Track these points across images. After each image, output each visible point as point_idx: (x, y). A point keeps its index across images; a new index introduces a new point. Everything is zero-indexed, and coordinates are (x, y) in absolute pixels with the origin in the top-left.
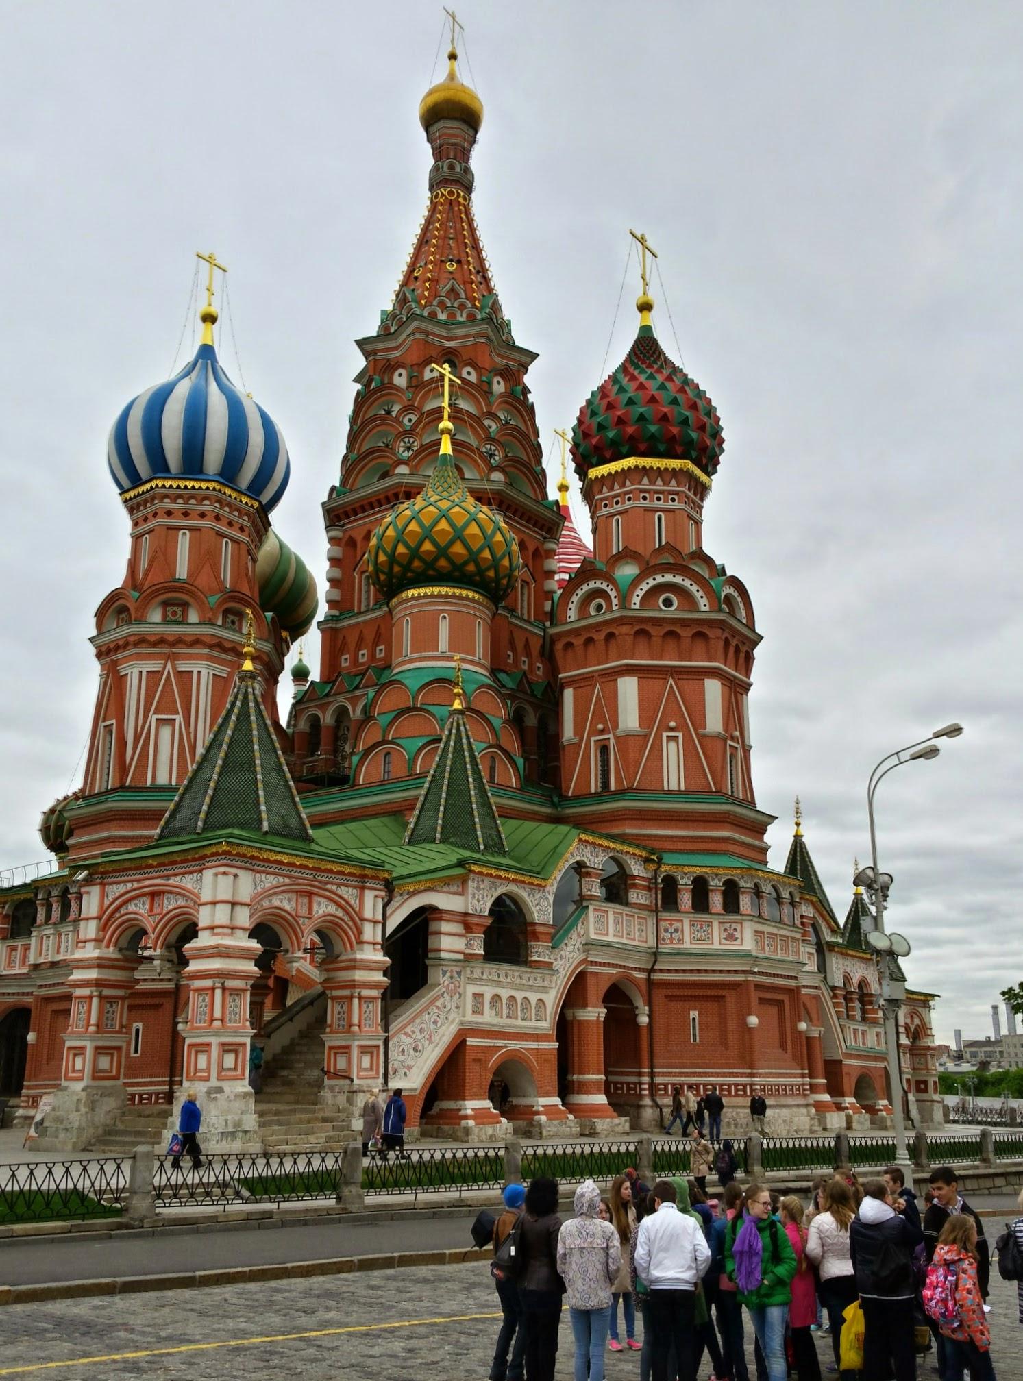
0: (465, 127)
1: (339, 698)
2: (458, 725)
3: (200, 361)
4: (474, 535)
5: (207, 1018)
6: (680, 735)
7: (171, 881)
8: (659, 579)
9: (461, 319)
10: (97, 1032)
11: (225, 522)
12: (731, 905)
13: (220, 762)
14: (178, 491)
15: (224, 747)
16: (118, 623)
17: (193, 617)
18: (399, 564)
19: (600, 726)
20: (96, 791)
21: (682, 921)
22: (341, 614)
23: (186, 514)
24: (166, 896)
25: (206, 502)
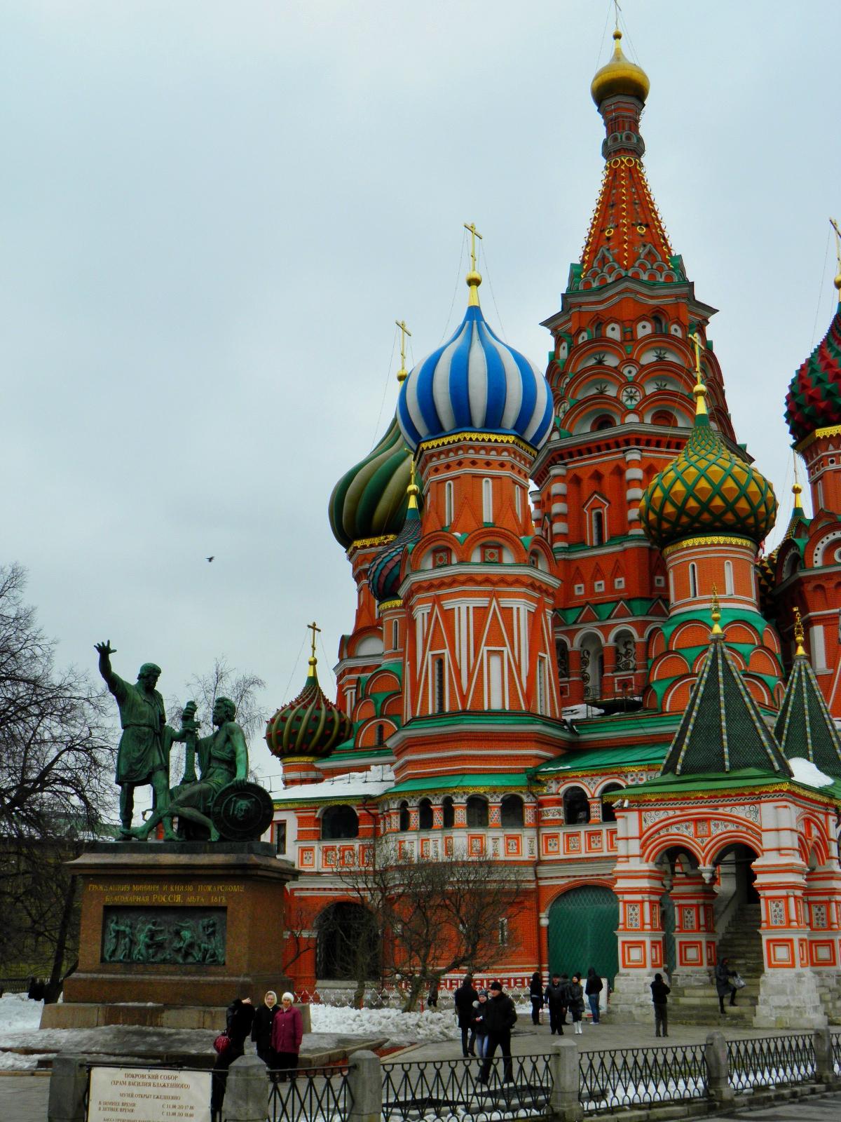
0: (637, 102)
2: (806, 669)
3: (475, 322)
4: (756, 492)
5: (784, 919)
7: (720, 810)
9: (662, 280)
10: (652, 929)
11: (517, 470)
13: (723, 711)
15: (722, 698)
18: (688, 515)
20: (430, 713)
23: (488, 464)
24: (712, 823)
25: (505, 453)
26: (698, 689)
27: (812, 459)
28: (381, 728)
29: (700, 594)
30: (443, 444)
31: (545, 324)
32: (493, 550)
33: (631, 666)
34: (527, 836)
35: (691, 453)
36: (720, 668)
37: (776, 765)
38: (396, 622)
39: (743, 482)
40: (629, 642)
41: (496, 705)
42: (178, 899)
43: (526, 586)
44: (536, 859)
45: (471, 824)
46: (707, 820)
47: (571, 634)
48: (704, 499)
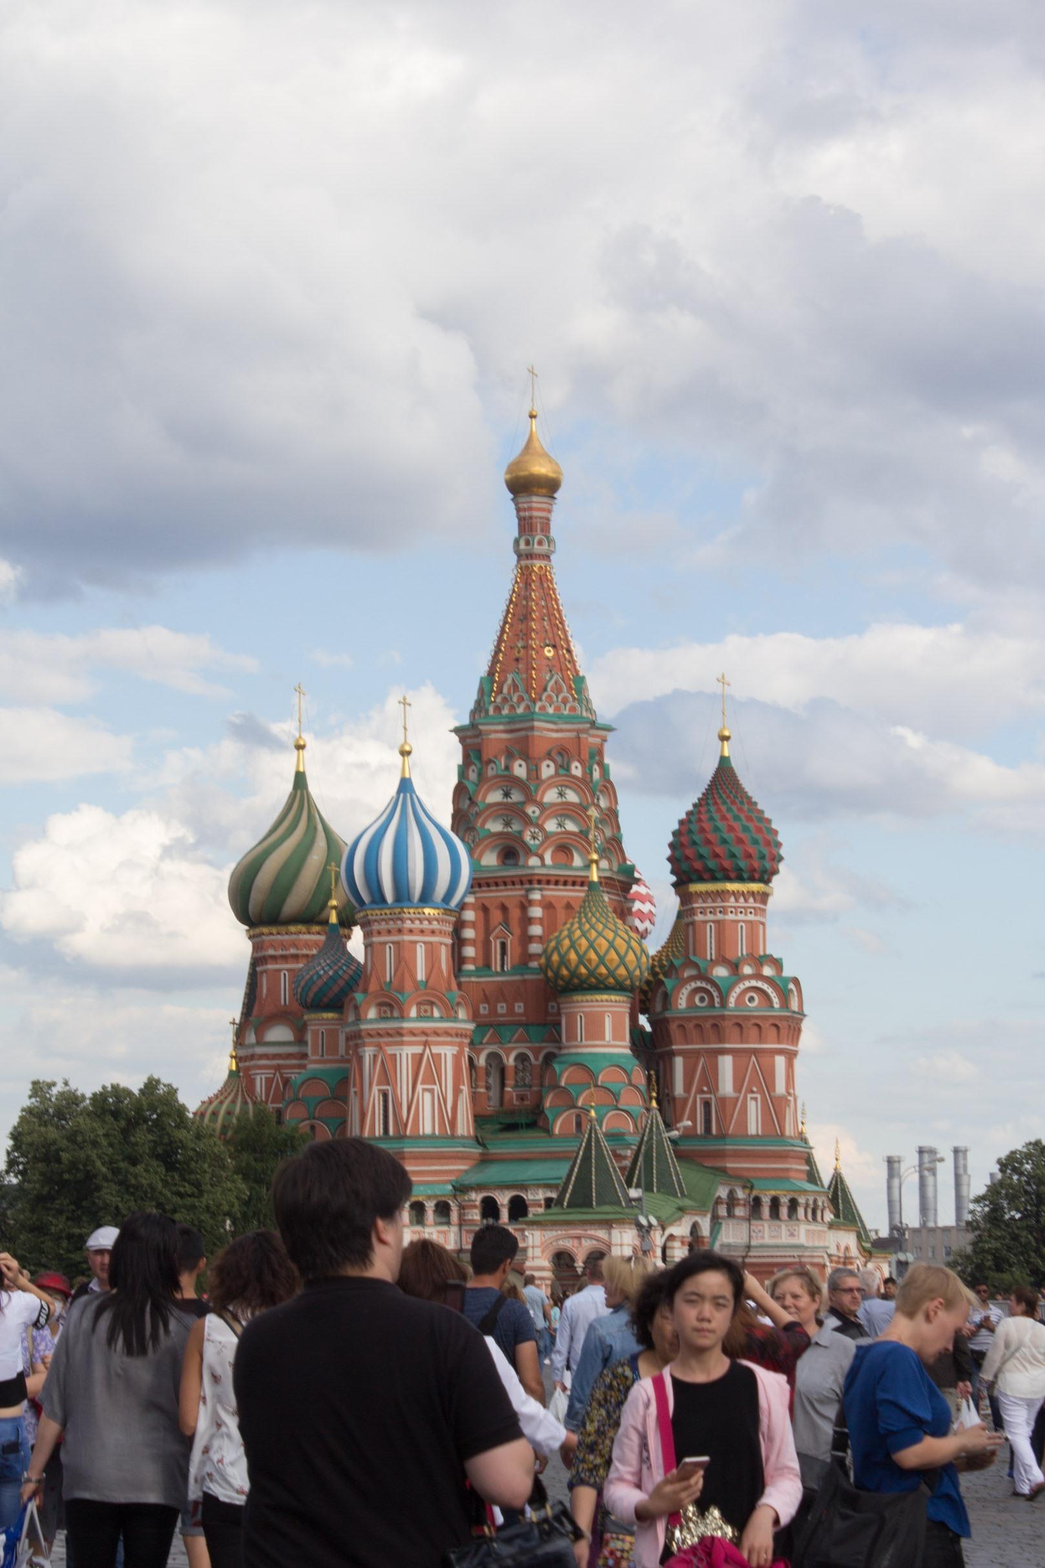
1: (492, 1047)
3: (408, 795)
4: (631, 961)
6: (759, 1096)
7: (589, 1232)
8: (747, 984)
9: (566, 712)
14: (418, 916)
16: (379, 1013)
17: (436, 1014)
18: (578, 978)
19: (705, 1089)
21: (763, 1226)
22: (476, 967)
23: (422, 931)
25: (435, 923)
26: (578, 1153)
27: (687, 905)
28: (313, 1127)
29: (586, 1040)
30: (386, 914)
31: (451, 731)
33: (527, 1081)
35: (584, 920)
36: (593, 1140)
38: (323, 1032)
39: (622, 953)
40: (526, 1060)
41: (428, 1130)
43: (451, 1035)
46: (579, 1238)
48: (591, 968)
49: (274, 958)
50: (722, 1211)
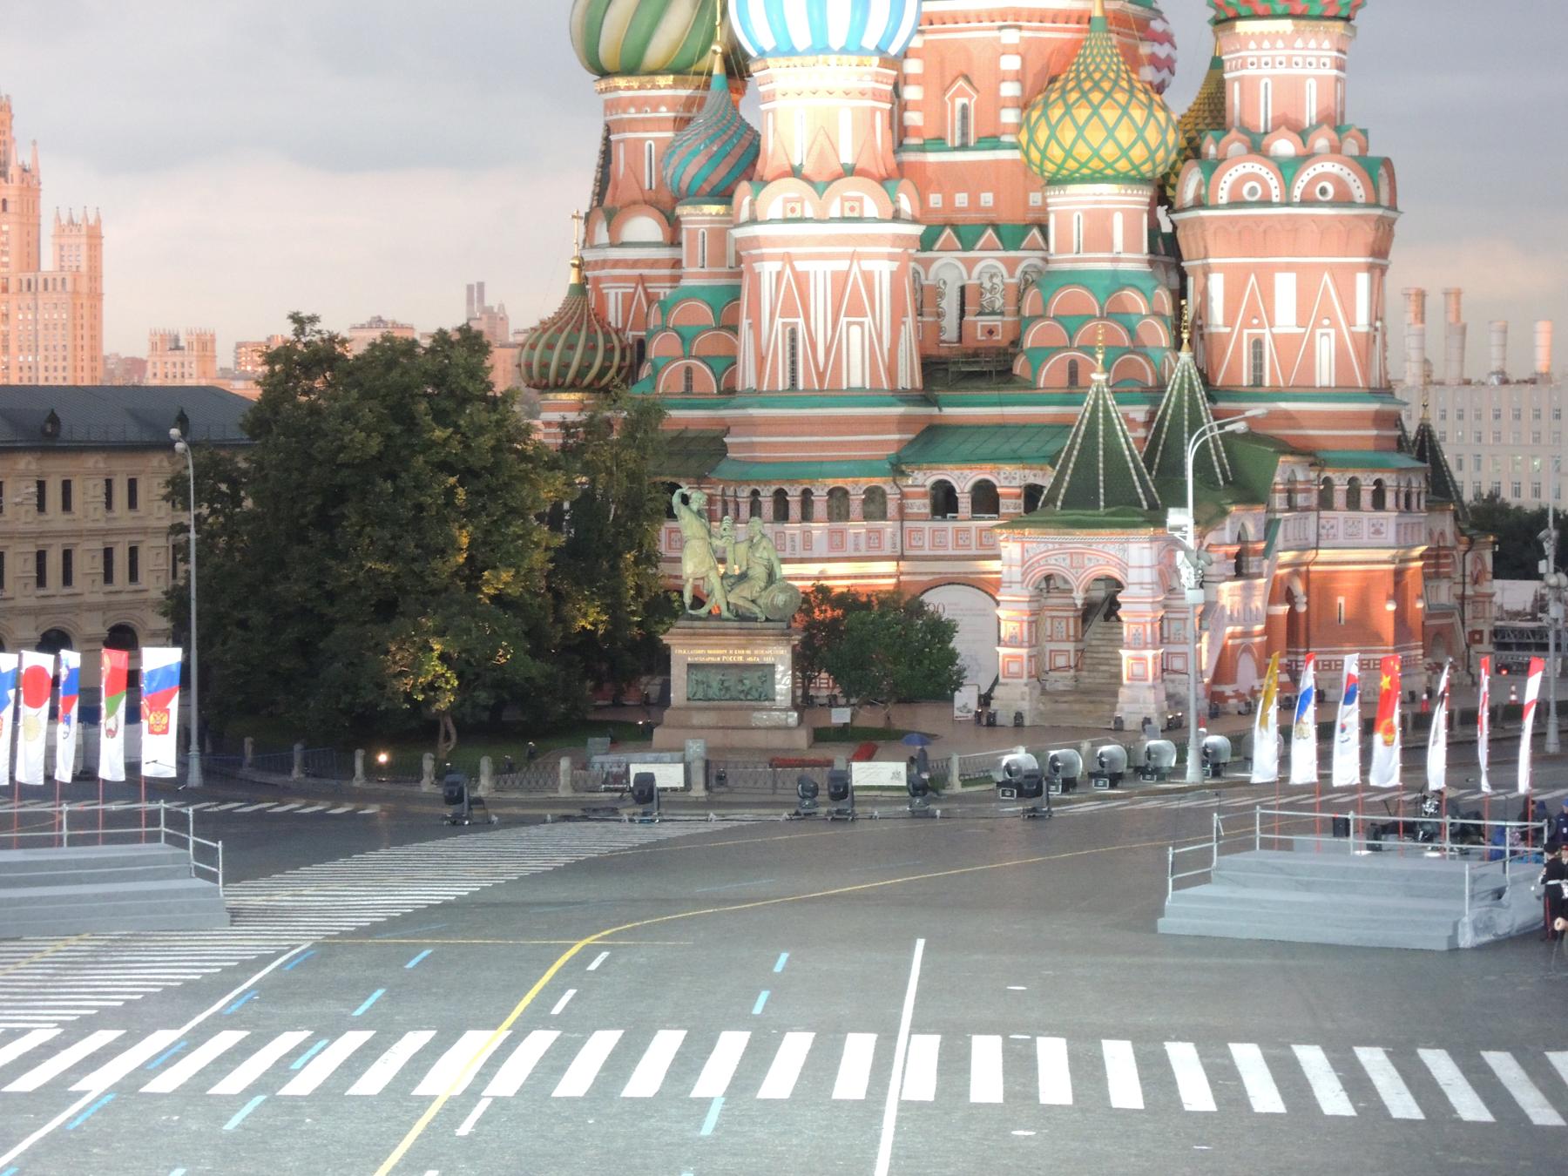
6: (1332, 332)
7: (1094, 547)
12: (1378, 502)
18: (1076, 160)
19: (1255, 321)
20: (780, 388)
24: (1087, 556)
27: (1232, 52)
28: (689, 370)
29: (1085, 251)
32: (852, 203)
34: (889, 527)
35: (1083, 75)
36: (1101, 408)
37: (1145, 503)
41: (856, 382)
42: (740, 659)
44: (899, 553)
45: (830, 519)
46: (1083, 554)
47: (927, 264)
49: (631, 125)
50: (1279, 500)
